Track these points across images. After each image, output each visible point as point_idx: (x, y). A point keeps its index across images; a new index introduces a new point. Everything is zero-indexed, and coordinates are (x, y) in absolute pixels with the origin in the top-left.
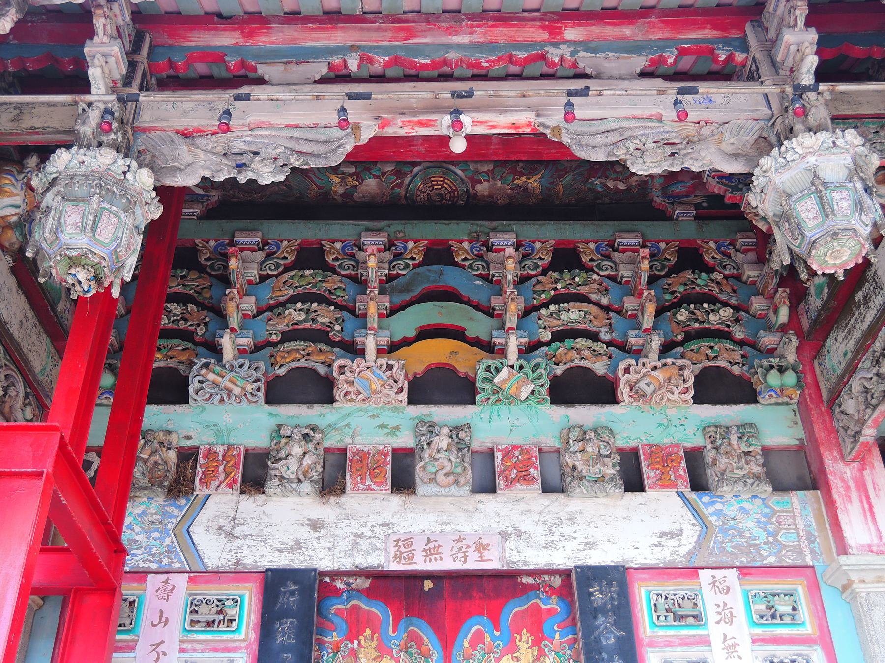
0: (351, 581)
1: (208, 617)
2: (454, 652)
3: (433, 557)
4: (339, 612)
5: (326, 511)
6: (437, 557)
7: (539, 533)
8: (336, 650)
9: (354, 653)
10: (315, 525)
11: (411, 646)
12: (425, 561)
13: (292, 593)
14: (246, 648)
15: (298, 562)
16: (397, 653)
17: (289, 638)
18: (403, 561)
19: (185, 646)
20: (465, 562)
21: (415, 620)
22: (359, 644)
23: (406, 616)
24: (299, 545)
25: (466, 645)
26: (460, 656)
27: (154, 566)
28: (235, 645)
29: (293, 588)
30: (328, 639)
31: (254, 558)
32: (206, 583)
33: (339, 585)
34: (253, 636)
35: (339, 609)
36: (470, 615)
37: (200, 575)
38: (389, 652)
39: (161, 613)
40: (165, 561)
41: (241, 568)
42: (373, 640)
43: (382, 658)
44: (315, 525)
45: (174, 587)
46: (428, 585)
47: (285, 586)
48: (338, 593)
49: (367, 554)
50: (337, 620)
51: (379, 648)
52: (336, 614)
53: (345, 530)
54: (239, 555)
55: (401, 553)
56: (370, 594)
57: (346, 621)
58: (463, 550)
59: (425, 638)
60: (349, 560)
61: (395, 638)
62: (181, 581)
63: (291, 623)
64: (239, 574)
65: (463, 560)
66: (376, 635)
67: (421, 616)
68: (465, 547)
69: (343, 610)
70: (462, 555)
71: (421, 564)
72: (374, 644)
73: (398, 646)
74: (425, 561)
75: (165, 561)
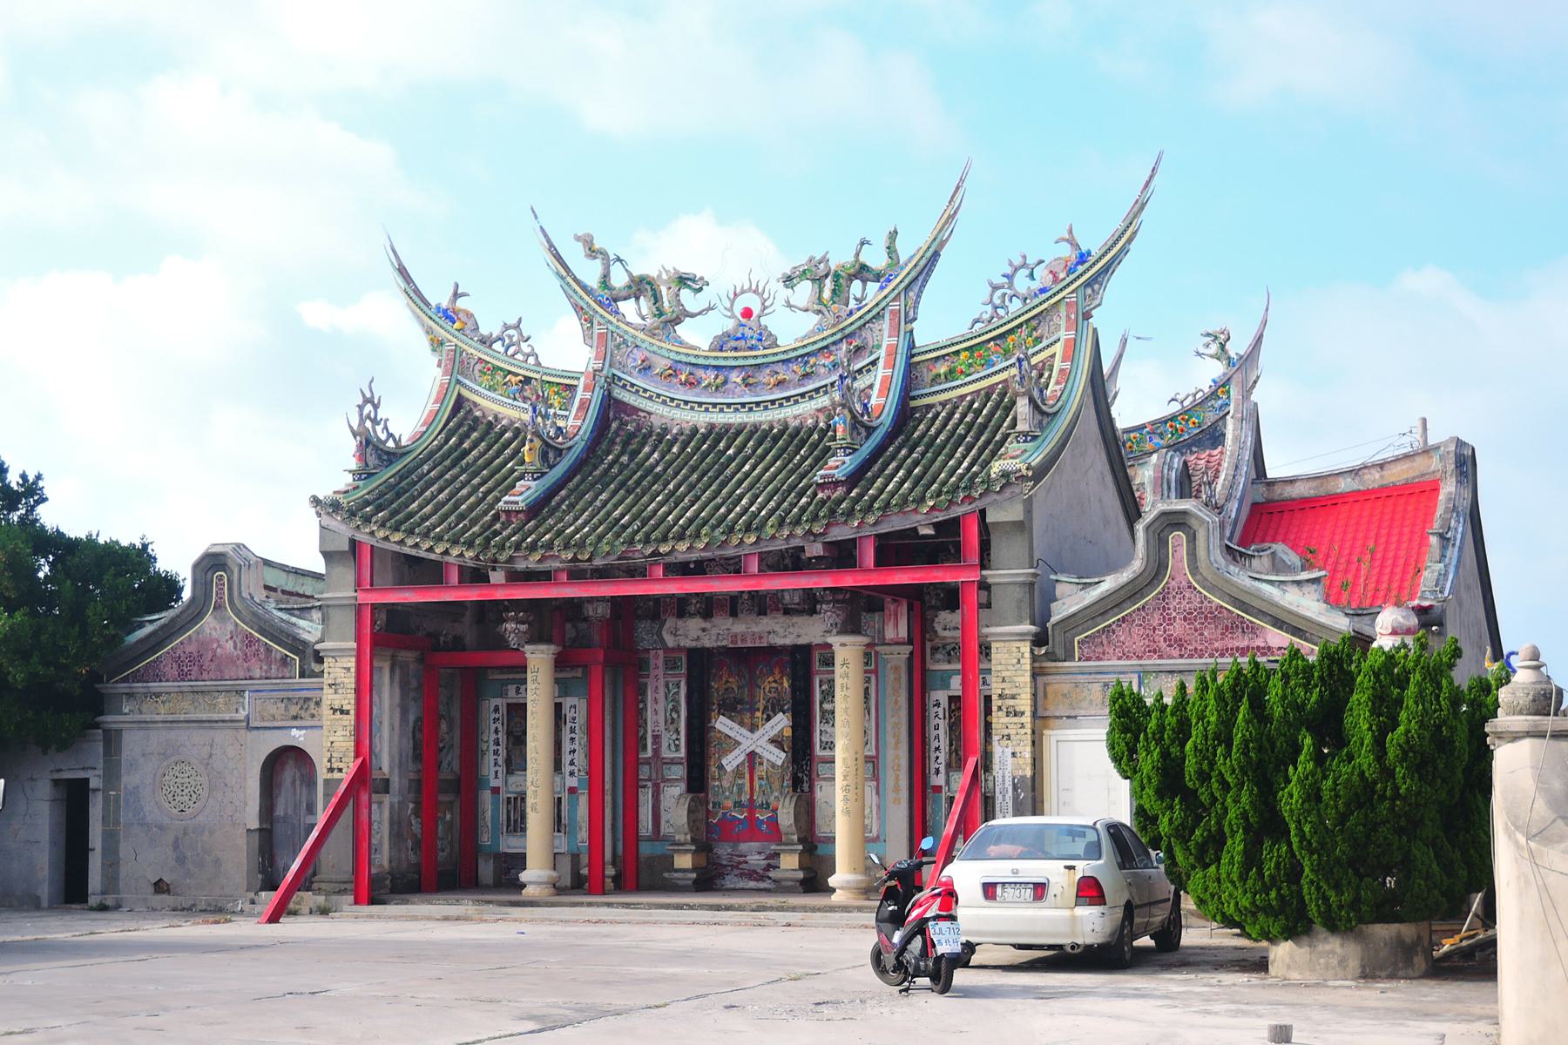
1: (671, 665)
5: (707, 625)
7: (781, 631)
10: (704, 630)
15: (699, 644)
24: (698, 639)
37: (667, 650)
44: (704, 630)
53: (714, 631)
62: (661, 652)
64: (679, 649)
71: (740, 645)
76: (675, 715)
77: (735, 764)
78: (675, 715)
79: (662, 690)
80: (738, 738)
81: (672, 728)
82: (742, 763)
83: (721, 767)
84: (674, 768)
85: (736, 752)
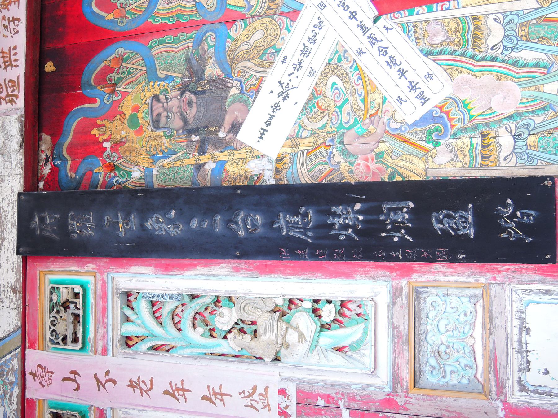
0: (43, 157)
2: (117, 29)
3: (13, 58)
4: (74, 168)
6: (13, 52)
8: (113, 167)
9: (116, 146)
11: (111, 80)
12: (17, 66)
13: (42, 220)
14: (102, 273)
16: (117, 96)
17: (88, 220)
18: (16, 93)
19: (100, 349)
20: (18, 19)
21: (84, 78)
22: (107, 141)
23: (80, 89)
25: (110, 16)
26: (122, 22)
27: (16, 391)
28: (99, 287)
29: (37, 219)
30: (101, 178)
31: (10, 271)
32: (35, 327)
33: (47, 170)
34: (90, 267)
35: (71, 168)
36: (81, 15)
38: (116, 105)
39: (65, 379)
40: (11, 378)
41: (19, 286)
42: (104, 125)
43: (121, 113)
45: (40, 366)
46: (50, 67)
47: (34, 230)
48: (55, 170)
49: (8, 136)
50: (82, 169)
51: (112, 118)
52: (76, 171)
54: (6, 289)
55: (8, 95)
56: (57, 134)
57: (83, 158)
58: (6, 23)
59: (103, 64)
60: (13, 156)
61: (102, 98)
63: (73, 219)
64: (25, 288)
65: (16, 22)
66: (98, 122)
67: (81, 72)
68: (4, 22)
69: (73, 163)
70: (12, 23)
72: (107, 123)
73: (110, 96)
74: (17, 66)
75: (11, 378)
76: (225, 319)
77: (417, 65)
78: (225, 319)
79: (144, 365)
80: (318, 59)
81: (271, 331)
82: (414, 32)
83: (436, 124)
84: (435, 336)
85: (373, 65)
